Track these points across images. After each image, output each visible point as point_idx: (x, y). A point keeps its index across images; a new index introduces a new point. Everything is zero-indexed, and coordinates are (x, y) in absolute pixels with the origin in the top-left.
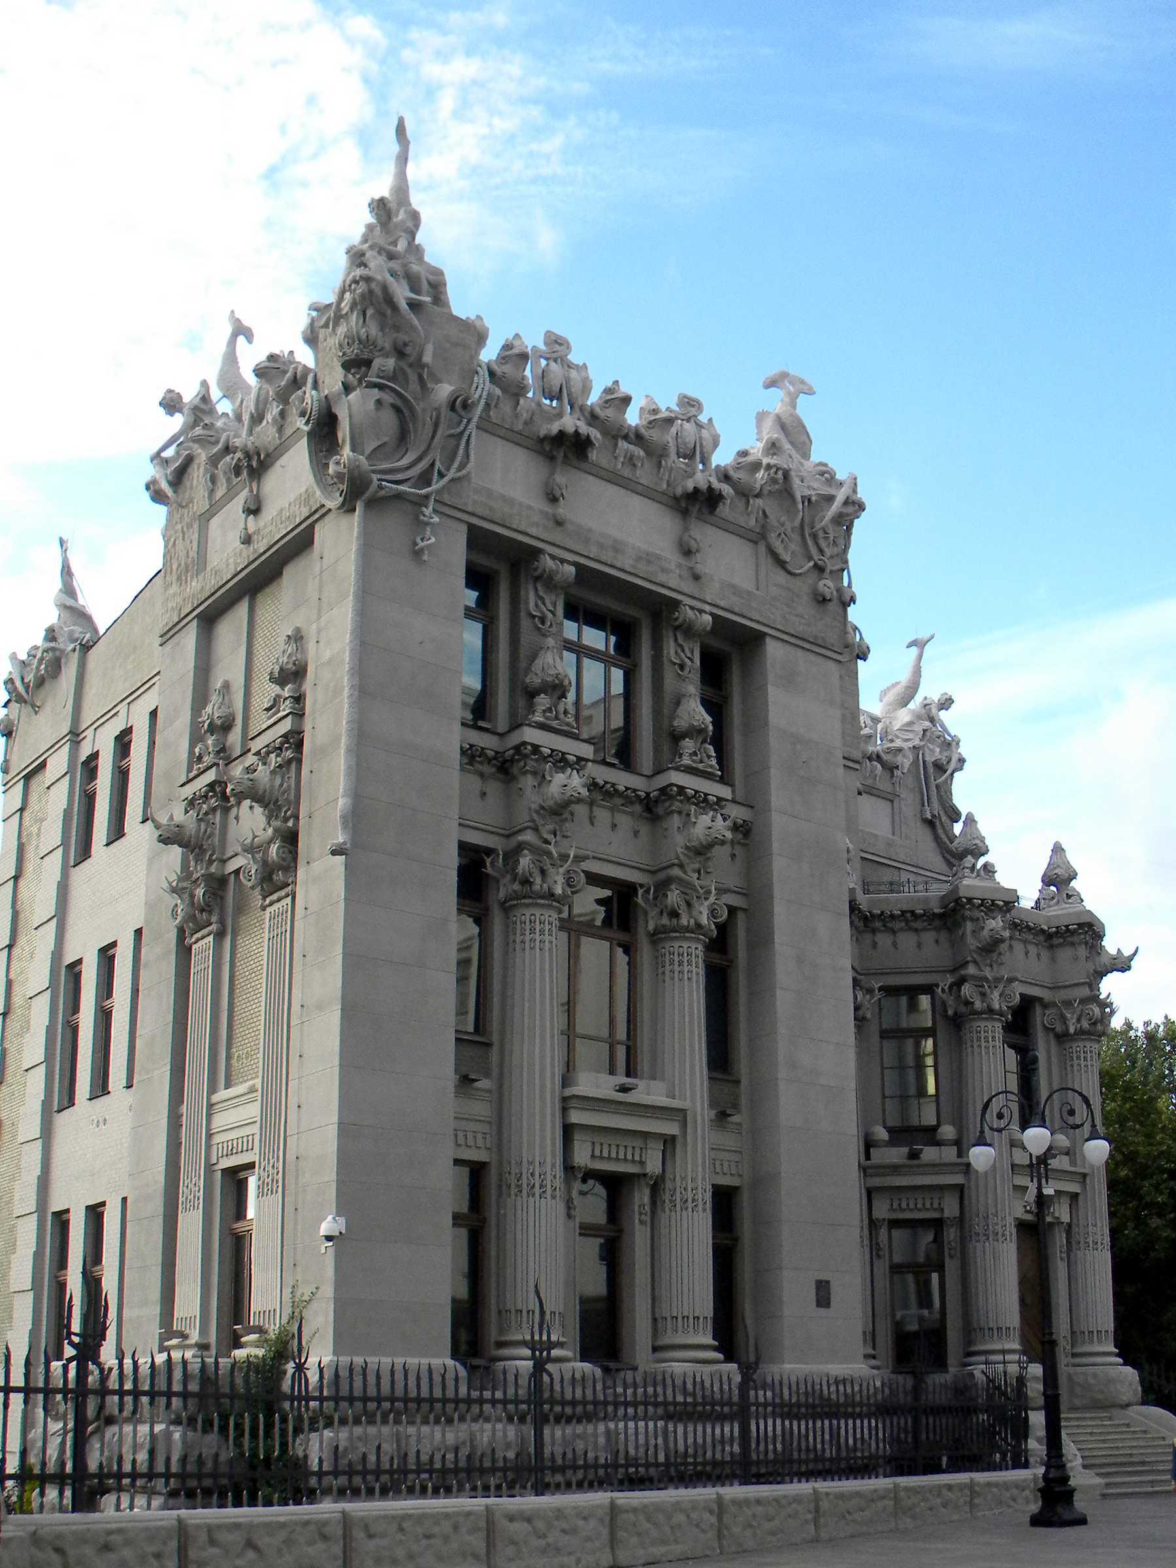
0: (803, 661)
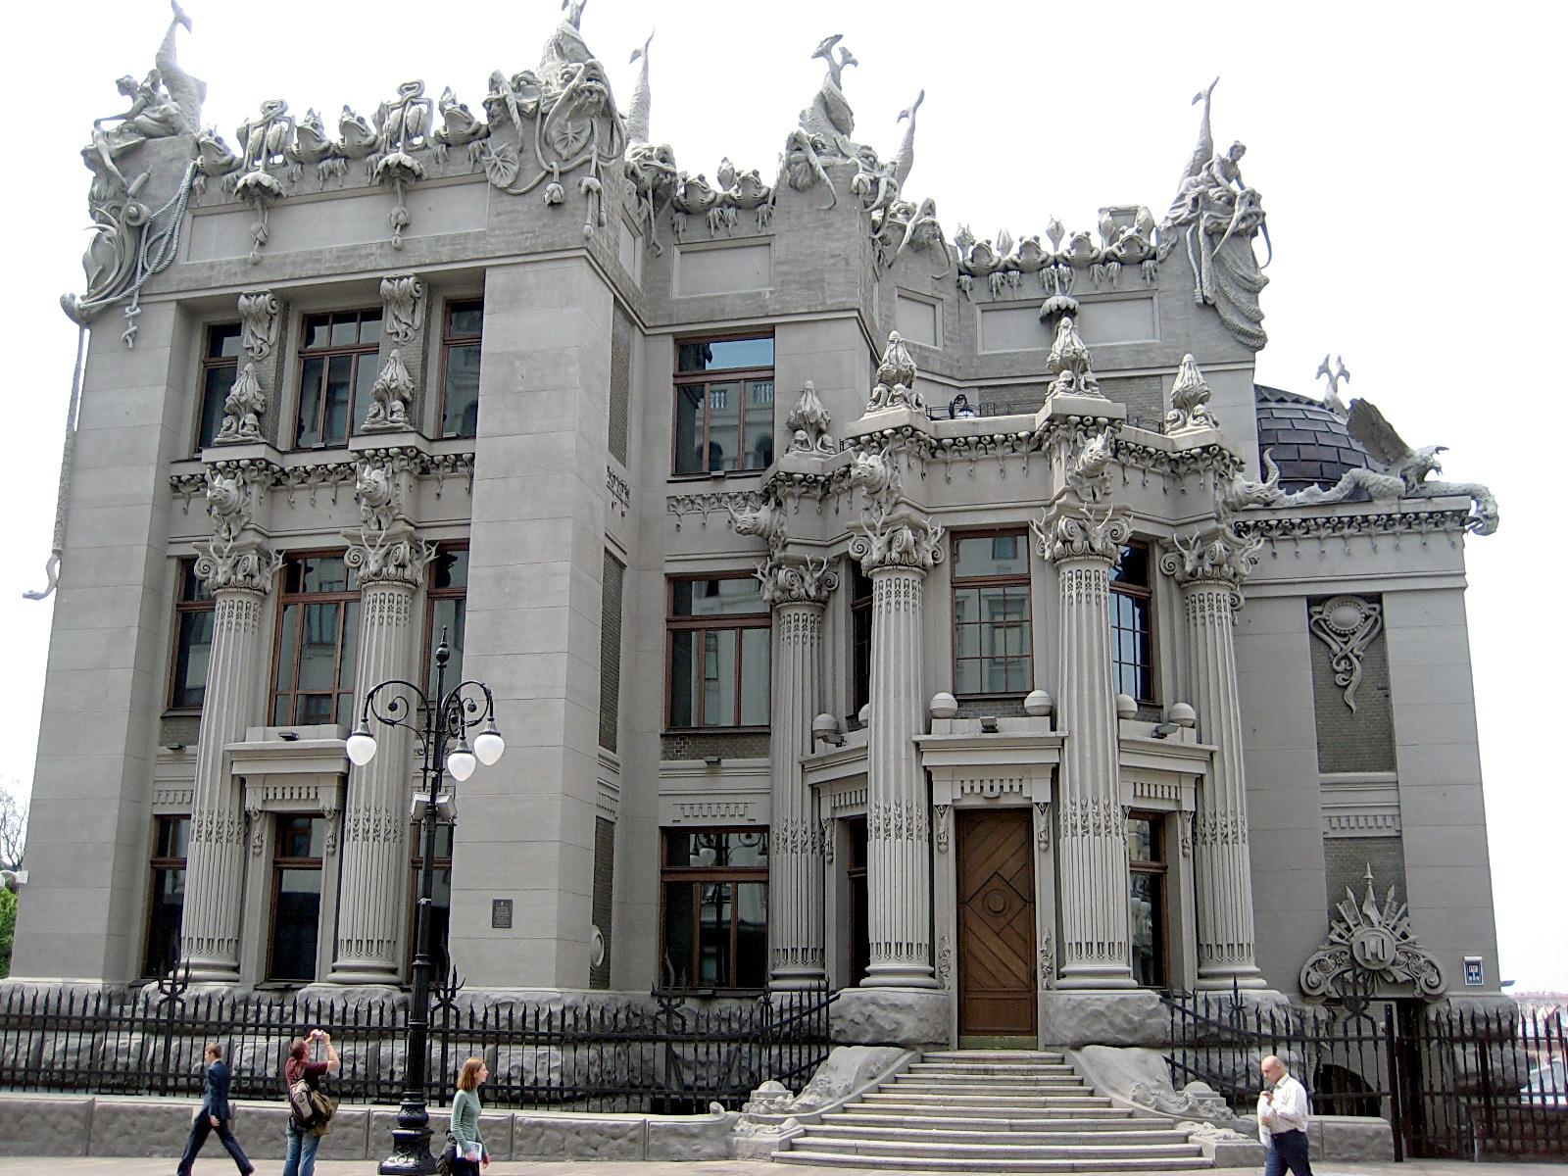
0: (530, 276)
